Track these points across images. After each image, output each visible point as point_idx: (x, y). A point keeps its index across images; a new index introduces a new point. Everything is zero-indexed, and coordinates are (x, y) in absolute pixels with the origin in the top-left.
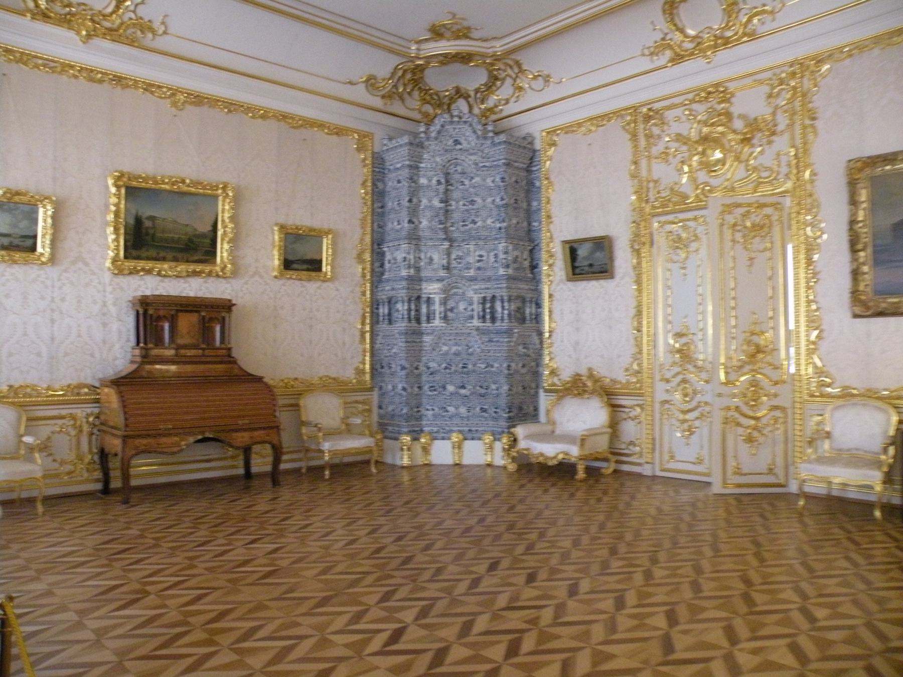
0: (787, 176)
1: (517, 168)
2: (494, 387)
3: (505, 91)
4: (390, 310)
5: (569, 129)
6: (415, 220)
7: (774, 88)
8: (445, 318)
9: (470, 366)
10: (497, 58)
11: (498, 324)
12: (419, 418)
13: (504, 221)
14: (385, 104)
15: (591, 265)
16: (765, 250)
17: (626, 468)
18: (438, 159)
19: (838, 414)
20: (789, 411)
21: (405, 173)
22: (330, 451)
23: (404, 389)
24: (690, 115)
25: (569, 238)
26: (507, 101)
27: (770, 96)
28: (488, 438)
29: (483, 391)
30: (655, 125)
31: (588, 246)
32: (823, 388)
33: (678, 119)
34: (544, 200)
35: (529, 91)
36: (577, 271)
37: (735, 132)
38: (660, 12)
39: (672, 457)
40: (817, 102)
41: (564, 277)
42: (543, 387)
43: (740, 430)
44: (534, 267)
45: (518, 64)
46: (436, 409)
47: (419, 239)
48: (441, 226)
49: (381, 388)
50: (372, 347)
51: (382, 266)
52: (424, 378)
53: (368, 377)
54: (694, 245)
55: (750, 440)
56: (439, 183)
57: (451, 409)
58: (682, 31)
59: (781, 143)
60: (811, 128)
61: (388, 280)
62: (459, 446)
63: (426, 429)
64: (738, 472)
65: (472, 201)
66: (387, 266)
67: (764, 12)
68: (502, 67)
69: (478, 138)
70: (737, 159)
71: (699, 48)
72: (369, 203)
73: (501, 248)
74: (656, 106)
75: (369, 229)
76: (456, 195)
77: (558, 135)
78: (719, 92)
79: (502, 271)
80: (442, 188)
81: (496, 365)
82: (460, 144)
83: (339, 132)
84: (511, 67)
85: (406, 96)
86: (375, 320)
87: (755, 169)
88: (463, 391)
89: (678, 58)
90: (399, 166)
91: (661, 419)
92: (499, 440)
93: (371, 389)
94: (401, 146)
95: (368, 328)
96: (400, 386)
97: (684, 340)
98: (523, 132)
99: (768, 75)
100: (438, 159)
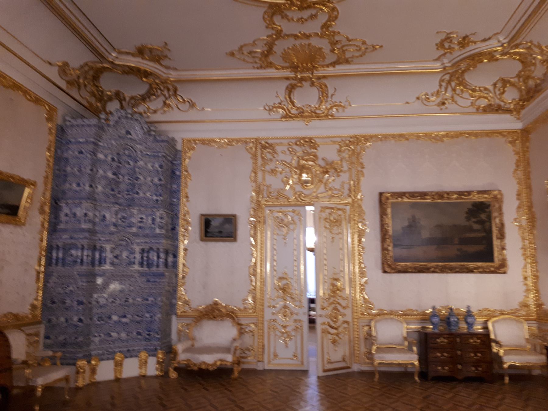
0: (349, 196)
1: (168, 160)
2: (147, 315)
3: (156, 104)
4: (64, 254)
5: (203, 142)
6: (94, 185)
7: (341, 147)
8: (112, 264)
9: (131, 301)
10: (165, 82)
11: (154, 269)
12: (88, 345)
13: (160, 195)
14: (67, 87)
15: (220, 232)
16: (340, 233)
17: (246, 366)
18: (113, 142)
19: (378, 325)
20: (351, 324)
21: (91, 147)
22: (42, 385)
23: (80, 320)
24: (293, 151)
25: (204, 213)
26: (155, 112)
27: (339, 151)
28: (143, 355)
29: (139, 319)
30: (269, 152)
31: (221, 220)
32: (369, 311)
33: (283, 152)
34: (183, 185)
35: (175, 109)
36: (208, 235)
37: (320, 166)
38: (284, 88)
39: (276, 356)
40: (364, 160)
41: (198, 238)
42: (176, 314)
43: (330, 336)
44: (173, 229)
45: (175, 90)
46: (102, 335)
47: (95, 200)
48: (112, 193)
49: (49, 321)
50: (45, 285)
51: (57, 217)
52: (95, 311)
53: (38, 312)
54: (291, 227)
55: (334, 342)
56: (113, 159)
57: (114, 334)
58: (293, 103)
59: (345, 177)
60: (360, 173)
61: (65, 231)
62: (119, 365)
63: (93, 353)
64: (330, 362)
65: (138, 178)
66: (63, 218)
67: (341, 106)
68: (162, 88)
69: (145, 133)
70: (320, 181)
71: (301, 114)
72: (51, 164)
73: (158, 214)
74: (269, 141)
75: (49, 186)
76: (123, 171)
77: (196, 144)
78: (310, 142)
79: (158, 231)
80: (115, 164)
81: (150, 299)
82: (130, 134)
83: (37, 101)
84: (169, 90)
85: (82, 87)
86: (49, 263)
87: (330, 189)
88: (124, 320)
89: (287, 116)
90: (81, 140)
91: (269, 333)
92: (154, 355)
93: (39, 323)
94: (89, 126)
95: (42, 269)
96: (75, 319)
97: (284, 282)
98: (171, 136)
99: (339, 140)
100: (113, 142)
